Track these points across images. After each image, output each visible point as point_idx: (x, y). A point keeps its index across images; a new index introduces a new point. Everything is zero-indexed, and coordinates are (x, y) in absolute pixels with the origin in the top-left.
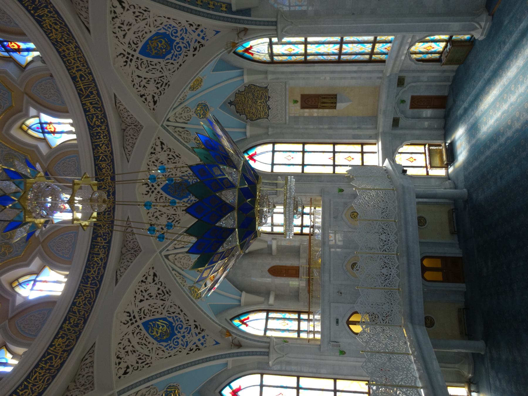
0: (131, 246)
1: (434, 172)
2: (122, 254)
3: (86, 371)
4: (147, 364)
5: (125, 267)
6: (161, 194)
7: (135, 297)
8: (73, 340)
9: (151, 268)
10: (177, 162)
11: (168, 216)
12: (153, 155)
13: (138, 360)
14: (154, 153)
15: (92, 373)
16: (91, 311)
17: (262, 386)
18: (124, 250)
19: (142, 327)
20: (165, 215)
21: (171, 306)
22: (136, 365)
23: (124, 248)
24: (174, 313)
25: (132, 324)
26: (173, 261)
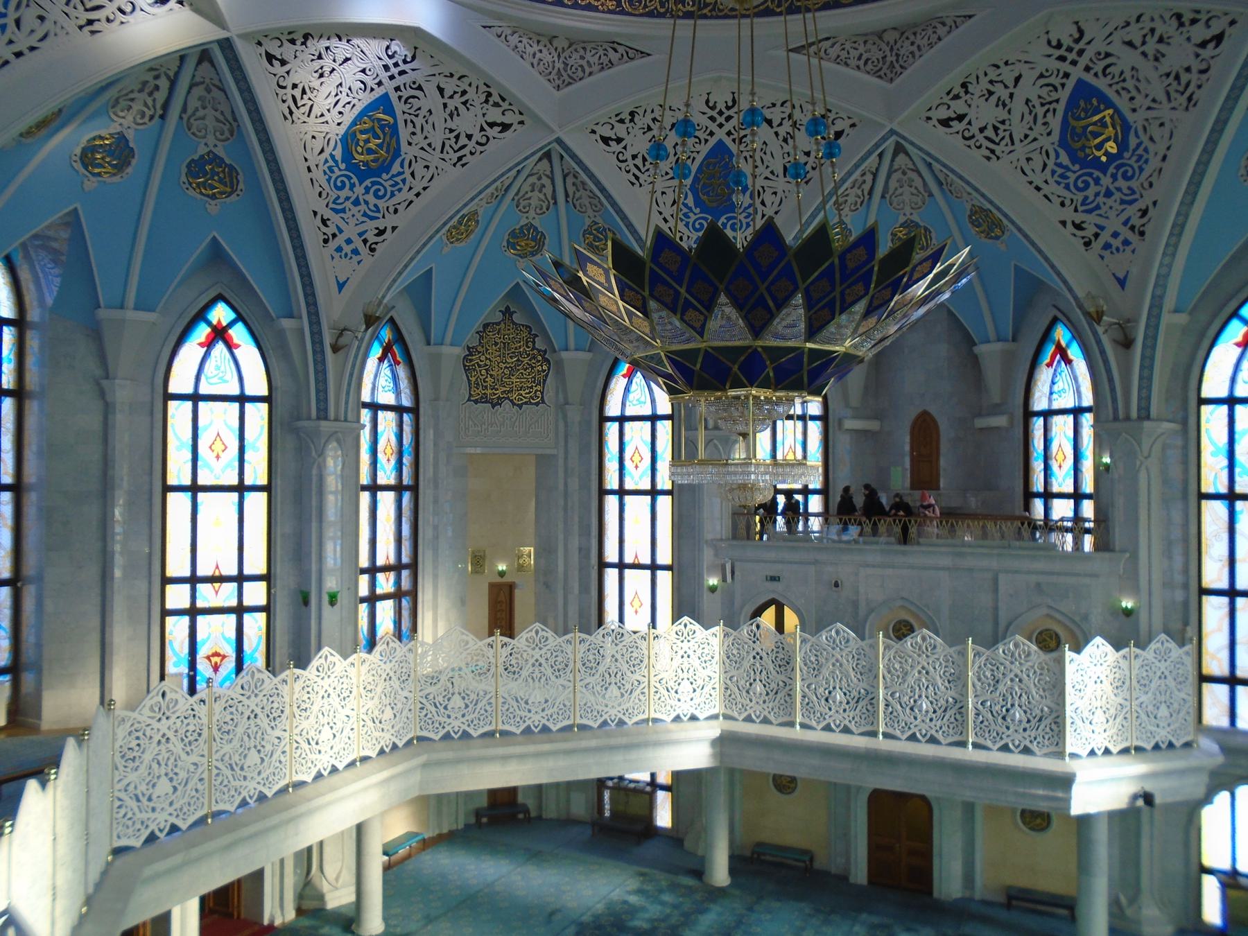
0: (902, 52)
1: (1211, 889)
2: (880, 35)
3: (592, 60)
4: (637, 178)
5: (844, 54)
6: (1063, 85)
7: (774, 105)
8: (646, 6)
9: (851, 122)
10: (1173, 104)
11: (1003, 122)
12: (1174, 23)
13: (640, 156)
14: (1181, 24)
15: (590, 74)
16: (717, 17)
17: (654, 418)
18: (890, 37)
19: (713, 141)
20: (1002, 114)
21: (775, 193)
22: (628, 155)
23: (896, 35)
24: (763, 203)
25: (712, 119)
26: (896, 167)
